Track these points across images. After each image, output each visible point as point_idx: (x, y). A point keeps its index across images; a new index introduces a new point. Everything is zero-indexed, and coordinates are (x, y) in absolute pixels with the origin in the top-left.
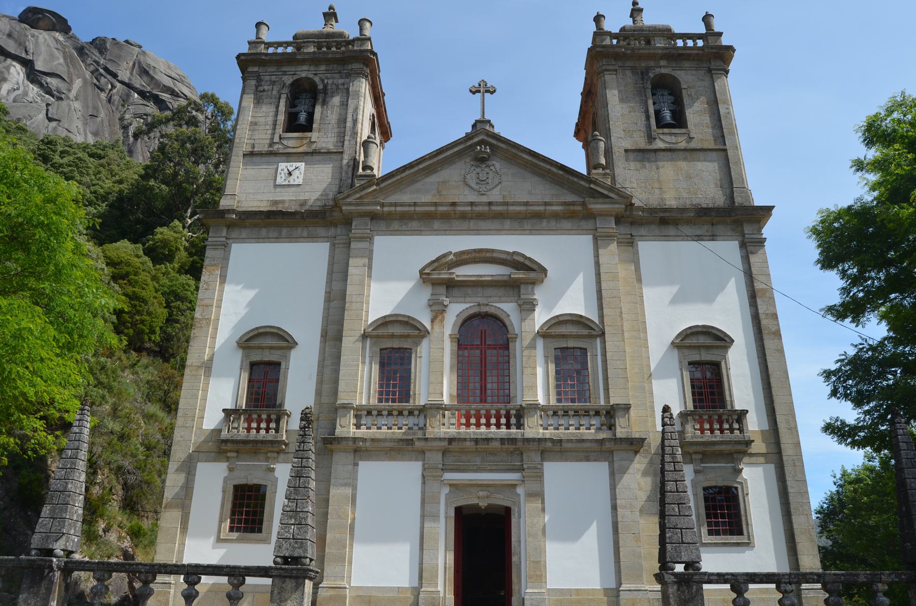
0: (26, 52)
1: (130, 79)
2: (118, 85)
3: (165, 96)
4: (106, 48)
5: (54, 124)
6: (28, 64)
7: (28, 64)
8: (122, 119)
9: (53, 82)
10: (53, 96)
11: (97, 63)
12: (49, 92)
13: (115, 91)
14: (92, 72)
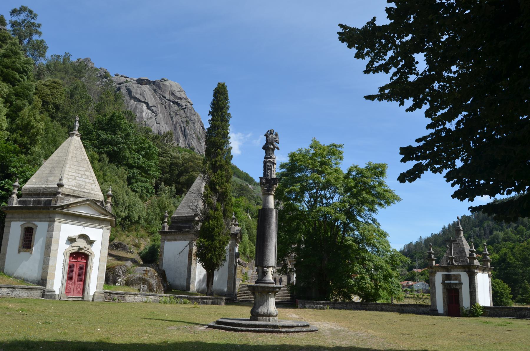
0: (145, 99)
1: (169, 98)
2: (167, 101)
3: (179, 101)
4: (161, 87)
5: (158, 125)
6: (147, 103)
7: (147, 103)
8: (170, 114)
9: (153, 108)
10: (154, 113)
11: (160, 94)
12: (153, 112)
13: (166, 104)
14: (159, 98)
